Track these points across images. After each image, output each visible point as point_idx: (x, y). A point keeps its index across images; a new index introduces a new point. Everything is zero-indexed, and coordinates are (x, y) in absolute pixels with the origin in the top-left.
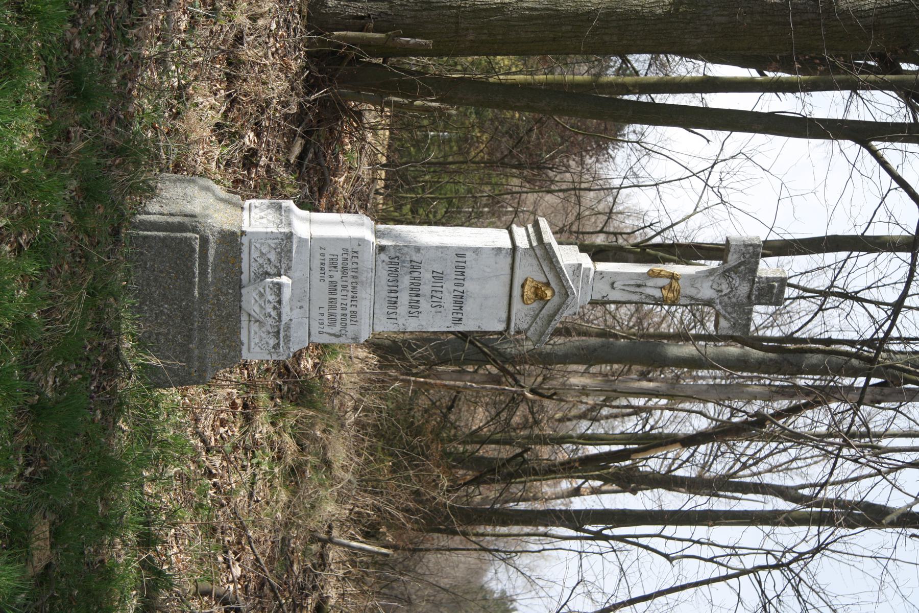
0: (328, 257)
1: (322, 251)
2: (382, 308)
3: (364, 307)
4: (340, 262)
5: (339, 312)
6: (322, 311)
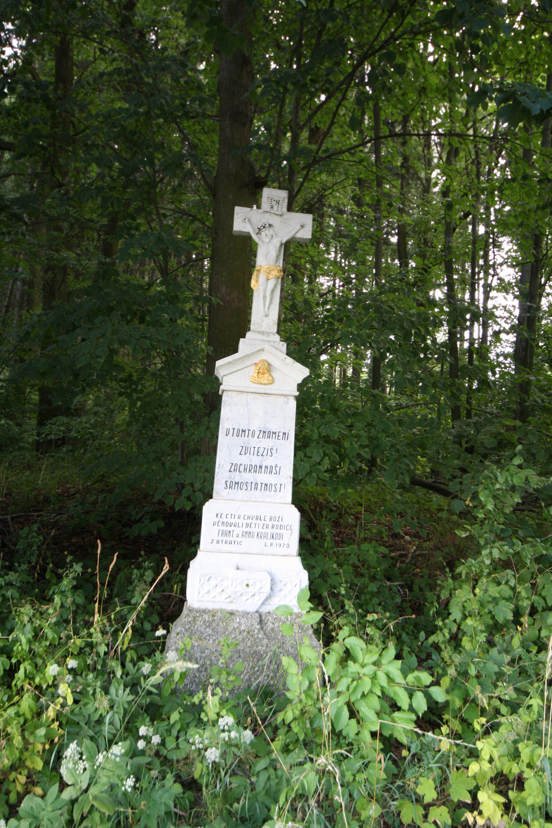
0: (220, 538)
1: (215, 542)
2: (269, 496)
3: (265, 511)
4: (225, 528)
5: (270, 531)
6: (268, 544)
